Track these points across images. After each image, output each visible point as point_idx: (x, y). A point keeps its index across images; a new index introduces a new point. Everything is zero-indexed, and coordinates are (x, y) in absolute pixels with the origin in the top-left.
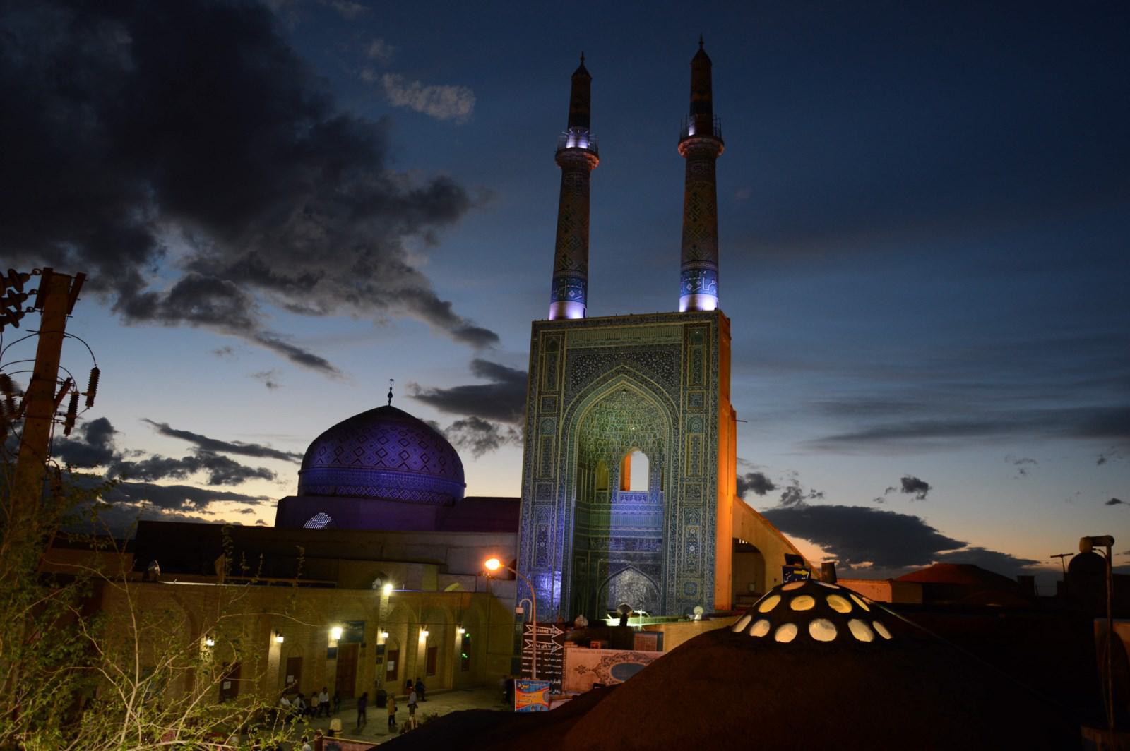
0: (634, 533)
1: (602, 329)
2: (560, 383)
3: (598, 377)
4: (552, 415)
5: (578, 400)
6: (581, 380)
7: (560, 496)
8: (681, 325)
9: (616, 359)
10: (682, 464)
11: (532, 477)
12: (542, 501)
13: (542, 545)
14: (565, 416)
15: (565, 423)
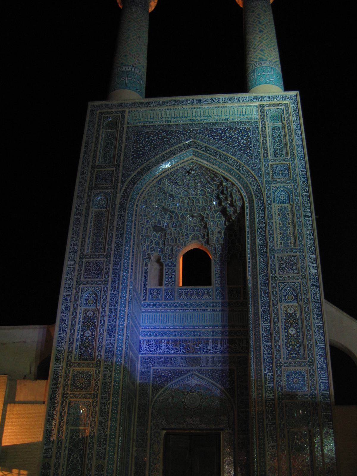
0: (196, 334)
1: (168, 109)
2: (119, 157)
3: (164, 151)
4: (107, 188)
5: (139, 173)
6: (143, 154)
7: (115, 274)
8: (256, 106)
9: (184, 134)
10: (271, 234)
11: (79, 253)
12: (90, 280)
13: (88, 333)
14: (124, 188)
15: (123, 196)
